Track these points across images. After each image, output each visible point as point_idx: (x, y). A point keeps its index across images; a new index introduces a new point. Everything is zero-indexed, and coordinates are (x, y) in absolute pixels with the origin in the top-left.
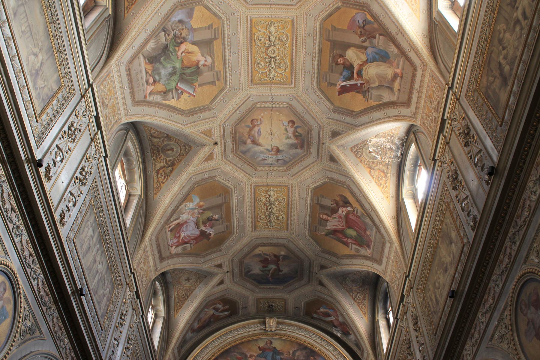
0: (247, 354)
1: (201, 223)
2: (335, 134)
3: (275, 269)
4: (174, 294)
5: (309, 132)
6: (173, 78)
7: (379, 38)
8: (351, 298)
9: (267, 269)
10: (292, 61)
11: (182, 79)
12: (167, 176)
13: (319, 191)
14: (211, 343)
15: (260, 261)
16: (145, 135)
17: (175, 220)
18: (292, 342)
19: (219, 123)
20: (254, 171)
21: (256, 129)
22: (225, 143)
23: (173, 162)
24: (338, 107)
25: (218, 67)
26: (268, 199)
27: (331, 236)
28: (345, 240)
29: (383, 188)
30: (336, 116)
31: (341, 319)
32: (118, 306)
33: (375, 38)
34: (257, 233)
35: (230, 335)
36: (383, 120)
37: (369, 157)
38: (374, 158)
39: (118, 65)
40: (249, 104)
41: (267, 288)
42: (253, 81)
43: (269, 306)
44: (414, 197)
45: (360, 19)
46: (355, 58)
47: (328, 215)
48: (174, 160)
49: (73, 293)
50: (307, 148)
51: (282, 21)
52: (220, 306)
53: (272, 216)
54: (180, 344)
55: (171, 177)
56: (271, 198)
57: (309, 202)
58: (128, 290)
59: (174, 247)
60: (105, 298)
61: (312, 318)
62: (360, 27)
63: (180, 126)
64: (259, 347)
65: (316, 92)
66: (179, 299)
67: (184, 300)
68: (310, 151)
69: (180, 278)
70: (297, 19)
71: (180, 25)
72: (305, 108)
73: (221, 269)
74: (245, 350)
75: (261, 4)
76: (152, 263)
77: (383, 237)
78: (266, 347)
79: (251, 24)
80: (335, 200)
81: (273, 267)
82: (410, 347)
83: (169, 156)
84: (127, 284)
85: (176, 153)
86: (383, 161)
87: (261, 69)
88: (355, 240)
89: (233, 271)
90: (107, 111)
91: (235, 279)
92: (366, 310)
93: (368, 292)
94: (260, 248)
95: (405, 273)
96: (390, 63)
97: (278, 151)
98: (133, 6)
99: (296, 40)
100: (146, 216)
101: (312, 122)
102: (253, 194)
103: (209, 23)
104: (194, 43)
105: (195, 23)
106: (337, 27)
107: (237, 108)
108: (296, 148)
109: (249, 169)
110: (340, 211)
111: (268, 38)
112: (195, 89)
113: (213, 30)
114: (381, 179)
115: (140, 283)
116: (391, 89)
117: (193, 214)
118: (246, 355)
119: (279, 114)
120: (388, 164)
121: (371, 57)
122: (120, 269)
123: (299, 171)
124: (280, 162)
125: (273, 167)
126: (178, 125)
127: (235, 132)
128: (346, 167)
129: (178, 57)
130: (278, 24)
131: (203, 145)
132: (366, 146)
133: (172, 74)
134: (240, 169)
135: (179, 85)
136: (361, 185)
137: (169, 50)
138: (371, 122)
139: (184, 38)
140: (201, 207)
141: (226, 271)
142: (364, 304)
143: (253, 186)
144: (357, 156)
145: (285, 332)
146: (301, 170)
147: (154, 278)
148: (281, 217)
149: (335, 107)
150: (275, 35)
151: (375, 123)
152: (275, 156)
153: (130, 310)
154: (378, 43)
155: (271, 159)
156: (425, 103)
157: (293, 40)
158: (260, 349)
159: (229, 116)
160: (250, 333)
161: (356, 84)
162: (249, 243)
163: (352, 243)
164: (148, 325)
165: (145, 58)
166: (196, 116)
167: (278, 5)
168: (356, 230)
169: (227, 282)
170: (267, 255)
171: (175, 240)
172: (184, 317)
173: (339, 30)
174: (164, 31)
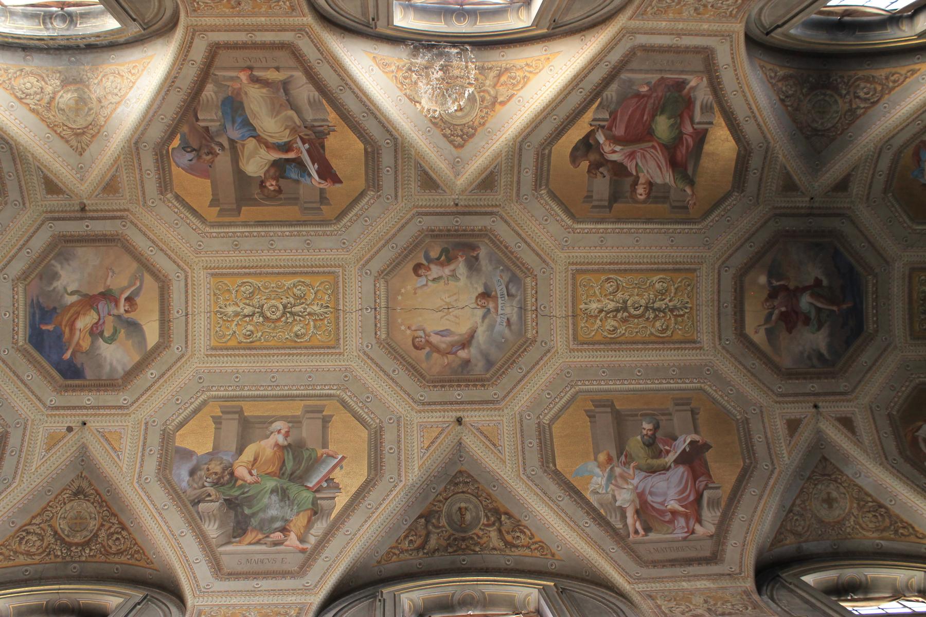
1: (656, 462)
2: (429, 182)
3: (812, 295)
4: (870, 538)
5: (435, 234)
6: (291, 496)
7: (204, 120)
8: (870, 112)
9: (813, 315)
10: (290, 273)
11: (300, 477)
12: (518, 526)
15: (790, 331)
16: (416, 561)
17: (624, 517)
19: (413, 413)
20: (538, 343)
21: (435, 339)
22: (462, 403)
23: (490, 510)
24: (367, 180)
25: (296, 408)
26: (611, 315)
27: (690, 172)
28: (690, 140)
29: (531, 72)
30: (387, 181)
36: (356, 90)
37: (472, 108)
38: (472, 99)
40: (379, 354)
42: (332, 346)
46: (257, 158)
47: (636, 183)
50: (472, 236)
51: (215, 295)
53: (656, 305)
55: (522, 518)
56: (597, 309)
57: (610, 226)
59: (698, 528)
62: (199, 157)
63: (398, 489)
65: (345, 226)
67: (890, 516)
68: (481, 230)
69: (820, 521)
70: (210, 268)
71: (199, 473)
72: (384, 246)
73: (805, 422)
75: (186, 331)
77: (631, 54)
79: (221, 349)
80: (589, 171)
81: (805, 301)
85: (471, 502)
86: (476, 79)
88: (681, 116)
91: (842, 389)
92: (903, 71)
93: (852, 73)
94: (749, 330)
96: (238, 94)
97: (486, 295)
99: (249, 267)
100: (583, 580)
101: (412, 230)
102: (596, 347)
103: (211, 421)
104: (240, 451)
106: (211, 197)
107: (385, 377)
108: (477, 258)
109: (533, 354)
111: (247, 319)
112: (329, 456)
114: (514, 78)
116: (285, 85)
119: (402, 295)
120: (482, 69)
121: (245, 130)
123: (534, 250)
124: (513, 290)
125: (526, 305)
126: (394, 493)
127: (440, 382)
128: (498, 155)
129: (257, 482)
130: (221, 302)
132: (446, 118)
133: (284, 495)
134: (528, 372)
136: (529, 118)
137: (236, 498)
138: (373, 113)
139: (224, 470)
140: (610, 460)
141: (814, 410)
142: (887, 78)
143: (575, 347)
144: (473, 135)
146: (529, 245)
148: (657, 286)
150: (242, 305)
151: (372, 107)
152: (500, 301)
155: (508, 309)
157: (249, 274)
159: (402, 394)
161: (308, 151)
162: (732, 356)
163: (692, 122)
165: (228, 543)
166: (387, 455)
167: (187, 302)
168: (653, 117)
169: (844, 409)
170: (771, 314)
171: (681, 521)
173: (215, 193)
174: (199, 502)
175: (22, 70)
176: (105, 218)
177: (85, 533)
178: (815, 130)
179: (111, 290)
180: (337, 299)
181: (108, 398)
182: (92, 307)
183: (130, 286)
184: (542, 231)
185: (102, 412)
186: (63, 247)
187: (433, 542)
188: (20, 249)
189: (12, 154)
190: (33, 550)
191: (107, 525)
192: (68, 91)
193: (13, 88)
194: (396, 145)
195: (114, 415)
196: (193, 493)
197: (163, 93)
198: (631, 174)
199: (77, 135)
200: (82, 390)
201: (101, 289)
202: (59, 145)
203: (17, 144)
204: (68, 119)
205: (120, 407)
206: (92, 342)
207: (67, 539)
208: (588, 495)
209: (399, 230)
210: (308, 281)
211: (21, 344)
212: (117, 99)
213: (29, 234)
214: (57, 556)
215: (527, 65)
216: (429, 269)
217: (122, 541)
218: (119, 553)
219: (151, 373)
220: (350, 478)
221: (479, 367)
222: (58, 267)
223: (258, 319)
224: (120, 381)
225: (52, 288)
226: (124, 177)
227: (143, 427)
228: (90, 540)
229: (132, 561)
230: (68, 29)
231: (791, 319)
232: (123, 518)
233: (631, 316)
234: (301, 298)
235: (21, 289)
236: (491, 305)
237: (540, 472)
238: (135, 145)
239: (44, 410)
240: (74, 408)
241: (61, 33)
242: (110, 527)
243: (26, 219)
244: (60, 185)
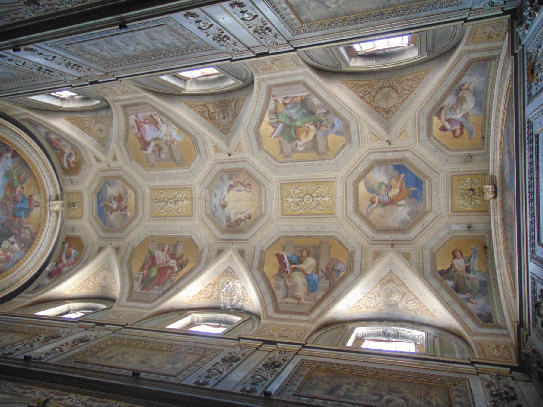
1: (157, 142)
2: (242, 253)
3: (112, 208)
4: (86, 117)
5: (242, 232)
7: (326, 283)
8: (89, 276)
9: (113, 201)
12: (201, 114)
13: (190, 242)
14: (35, 150)
15: (120, 194)
16: (238, 95)
17: (161, 120)
18: (39, 225)
19: (247, 157)
21: (243, 188)
22: (230, 162)
25: (295, 156)
27: (149, 255)
28: (146, 267)
31: (65, 269)
32: (87, 63)
33: (327, 279)
34: (147, 190)
35: (43, 168)
36: (259, 292)
37: (223, 283)
39: (303, 74)
40: (265, 182)
41: (93, 201)
42: (283, 185)
43: (73, 203)
44: (192, 324)
45: (340, 266)
47: (168, 251)
48: (215, 120)
49: (122, 18)
52: (73, 158)
53: (164, 203)
54: (33, 121)
58: (101, 74)
59: (135, 118)
60: (98, 51)
61: (64, 243)
62: (333, 267)
63: (246, 125)
64: (32, 196)
66: (81, 121)
69: (102, 123)
74: (28, 182)
76: (122, 97)
77: (154, 300)
78: (33, 202)
81: (115, 206)
82: (53, 338)
83: (218, 115)
84: (107, 73)
86: (221, 295)
87: (293, 191)
89: (110, 170)
90: (269, 63)
92: (76, 291)
95: (127, 324)
96: (308, 293)
97: (224, 206)
98: (347, 87)
99: (318, 218)
101: (250, 234)
104: (315, 137)
105: (331, 137)
108: (227, 222)
109: (206, 183)
110: (173, 261)
113: (325, 151)
115: (105, 86)
116: (287, 296)
117: (167, 136)
118: (23, 183)
120: (218, 299)
122: (122, 68)
124: (214, 208)
127: (239, 171)
128: (214, 263)
129: (304, 123)
131: (228, 144)
132: (233, 279)
133: (291, 119)
135: (281, 124)
137: (311, 116)
138: (256, 282)
139: (320, 128)
140: (173, 142)
142: (82, 289)
145: (48, 219)
147: (107, 99)
148: (164, 211)
149: (265, 251)
150: (322, 201)
153: (79, 75)
154: (323, 283)
156: (282, 325)
157: (318, 215)
158: (31, 196)
160: (46, 187)
161: (286, 268)
163: (144, 274)
164: (54, 92)
165: (307, 96)
167: (346, 202)
168: (156, 276)
169: (99, 166)
172: (61, 125)
174: (326, 113)
175: (415, 312)
176: (382, 240)
177: (383, 93)
178: (108, 270)
179: (382, 207)
180: (281, 204)
181: (380, 157)
182: (391, 199)
183: (372, 209)
184: (202, 233)
185: (382, 150)
186: (405, 228)
187: (233, 105)
188: (427, 226)
189: (423, 272)
190: (406, 82)
191: (371, 98)
192: (395, 301)
193: (419, 304)
194: (251, 269)
195: (376, 149)
196: (330, 116)
197: (341, 296)
198: (169, 255)
199: (392, 280)
200: (394, 159)
201: (387, 207)
202: (401, 276)
203: (419, 277)
204: (396, 287)
205: (373, 152)
206: (390, 182)
207: (391, 89)
208: (176, 128)
209: (255, 233)
210: (293, 212)
211: (427, 181)
212: (369, 296)
213: (422, 233)
214: (395, 80)
215: (199, 299)
216: (245, 217)
217: (362, 91)
218: (363, 86)
219: (361, 169)
220: (266, 128)
221: (225, 178)
222: (408, 218)
223: (314, 195)
224: (375, 164)
225: (412, 208)
226: (370, 259)
227: (361, 144)
228: (379, 90)
229: (355, 82)
230: (386, 329)
231: (119, 199)
232: (362, 102)
233: (172, 199)
234: (297, 205)
235: (428, 207)
236: (222, 202)
237: (196, 136)
238: (362, 272)
239: (411, 149)
240: (396, 151)
241: (390, 328)
242: (370, 97)
243: (421, 242)
244: (402, 257)
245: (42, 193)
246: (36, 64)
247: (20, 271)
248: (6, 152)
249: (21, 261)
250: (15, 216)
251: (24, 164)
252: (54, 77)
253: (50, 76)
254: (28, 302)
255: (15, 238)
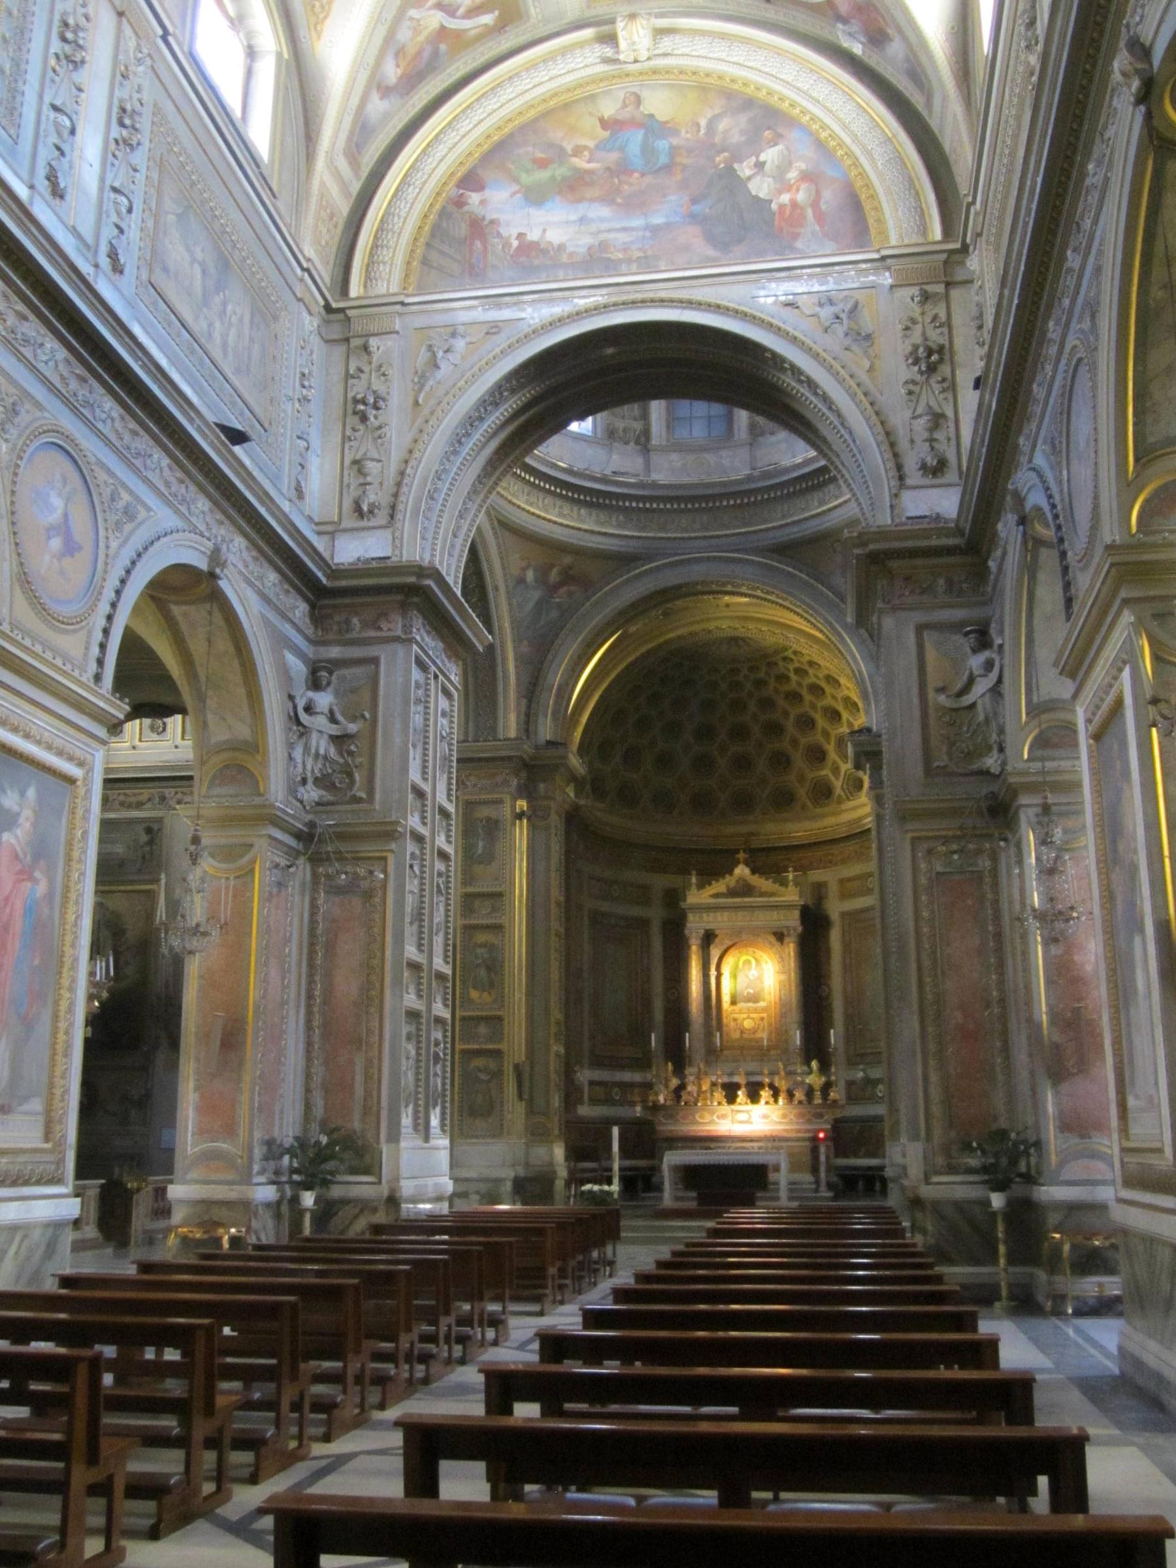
0: (564, 144)
14: (450, 123)
18: (703, 89)
35: (508, 93)
54: (349, 139)
74: (557, 135)
118: (562, 150)
153: (105, 20)
158: (604, 123)
172: (342, 49)
245: (591, 89)
246: (108, 158)
247: (855, 138)
248: (466, 208)
249: (823, 135)
250: (668, 168)
251: (497, 154)
252: (145, 97)
253: (147, 112)
254: (956, 107)
255: (741, 162)
